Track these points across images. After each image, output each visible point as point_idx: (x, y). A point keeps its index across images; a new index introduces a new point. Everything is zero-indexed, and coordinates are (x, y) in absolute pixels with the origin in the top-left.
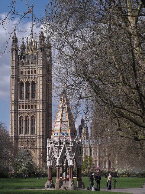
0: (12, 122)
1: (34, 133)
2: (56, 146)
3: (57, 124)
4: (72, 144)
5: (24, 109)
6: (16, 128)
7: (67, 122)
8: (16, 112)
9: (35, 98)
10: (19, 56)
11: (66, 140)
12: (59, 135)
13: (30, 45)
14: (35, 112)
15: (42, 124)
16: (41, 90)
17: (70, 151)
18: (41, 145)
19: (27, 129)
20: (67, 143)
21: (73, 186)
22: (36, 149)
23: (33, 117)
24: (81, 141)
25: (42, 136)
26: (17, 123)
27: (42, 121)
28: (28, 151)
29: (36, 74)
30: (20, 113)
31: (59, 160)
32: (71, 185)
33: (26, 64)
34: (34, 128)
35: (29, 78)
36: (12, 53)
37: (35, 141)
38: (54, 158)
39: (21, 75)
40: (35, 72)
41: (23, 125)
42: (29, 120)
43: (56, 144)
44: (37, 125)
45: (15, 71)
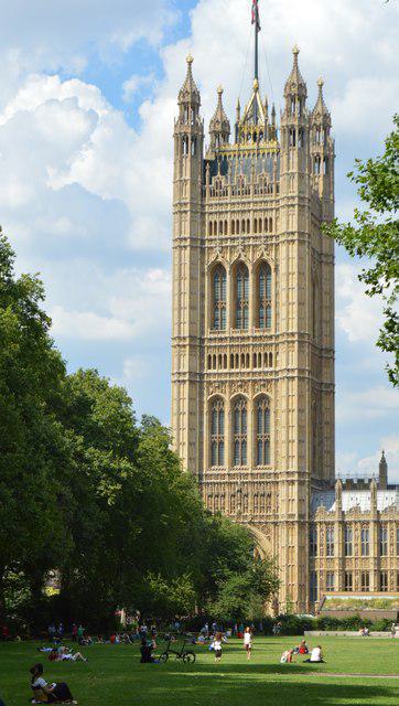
0: (178, 420)
8: (196, 380)
10: (205, 162)
13: (246, 119)
14: (268, 381)
15: (296, 429)
18: (295, 511)
19: (239, 447)
23: (261, 399)
25: (299, 473)
26: (201, 423)
27: (295, 414)
30: (210, 383)
34: (267, 442)
35: (245, 248)
36: (179, 151)
37: (269, 496)
39: (213, 237)
40: (269, 223)
41: (221, 431)
44: (276, 432)
45: (191, 221)
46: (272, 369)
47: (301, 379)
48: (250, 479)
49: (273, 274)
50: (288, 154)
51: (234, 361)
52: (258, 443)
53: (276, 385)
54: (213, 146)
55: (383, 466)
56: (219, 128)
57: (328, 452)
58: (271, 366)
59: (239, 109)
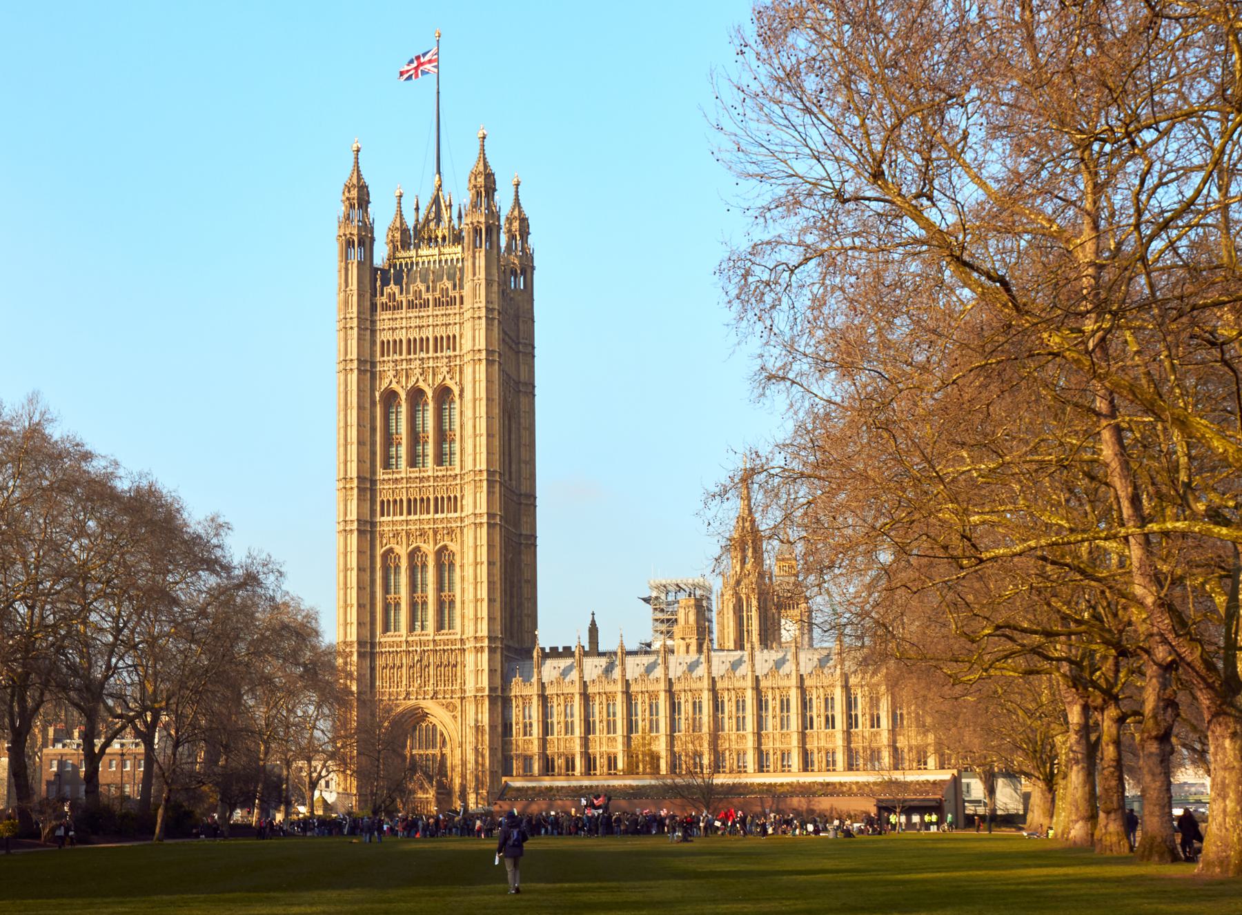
0: (346, 577)
6: (365, 606)
8: (367, 529)
10: (377, 269)
13: (427, 221)
18: (485, 684)
26: (373, 582)
27: (485, 567)
29: (457, 353)
33: (411, 305)
34: (452, 603)
37: (455, 666)
39: (386, 358)
40: (451, 341)
45: (359, 339)
46: (458, 514)
47: (490, 526)
50: (474, 257)
51: (412, 506)
52: (440, 604)
53: (462, 532)
55: (593, 631)
57: (529, 616)
58: (455, 511)
59: (417, 209)
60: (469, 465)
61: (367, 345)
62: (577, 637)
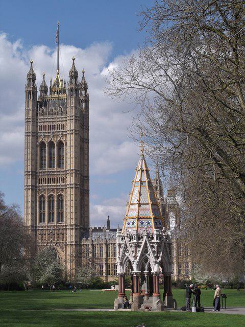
1: (62, 221)
2: (132, 242)
3: (132, 207)
4: (157, 239)
5: (46, 185)
6: (34, 214)
7: (148, 204)
8: (34, 188)
9: (63, 167)
11: (147, 233)
12: (136, 224)
13: (54, 85)
14: (63, 189)
16: (73, 155)
17: (154, 249)
18: (74, 240)
20: (150, 237)
21: (160, 305)
22: (66, 245)
23: (60, 196)
24: (170, 234)
25: (75, 225)
26: (36, 206)
27: (74, 202)
28: (54, 249)
30: (39, 190)
31: (137, 264)
32: (157, 304)
33: (49, 114)
34: (63, 213)
35: (54, 136)
37: (63, 234)
38: (129, 261)
39: (41, 132)
40: (63, 126)
42: (53, 201)
43: (131, 238)
44: (66, 209)
45: (32, 125)
48: (55, 228)
49: (65, 146)
50: (71, 99)
54: (41, 96)
55: (108, 222)
56: (43, 89)
59: (51, 81)
60: (68, 168)
61: (35, 127)
62: (103, 225)
